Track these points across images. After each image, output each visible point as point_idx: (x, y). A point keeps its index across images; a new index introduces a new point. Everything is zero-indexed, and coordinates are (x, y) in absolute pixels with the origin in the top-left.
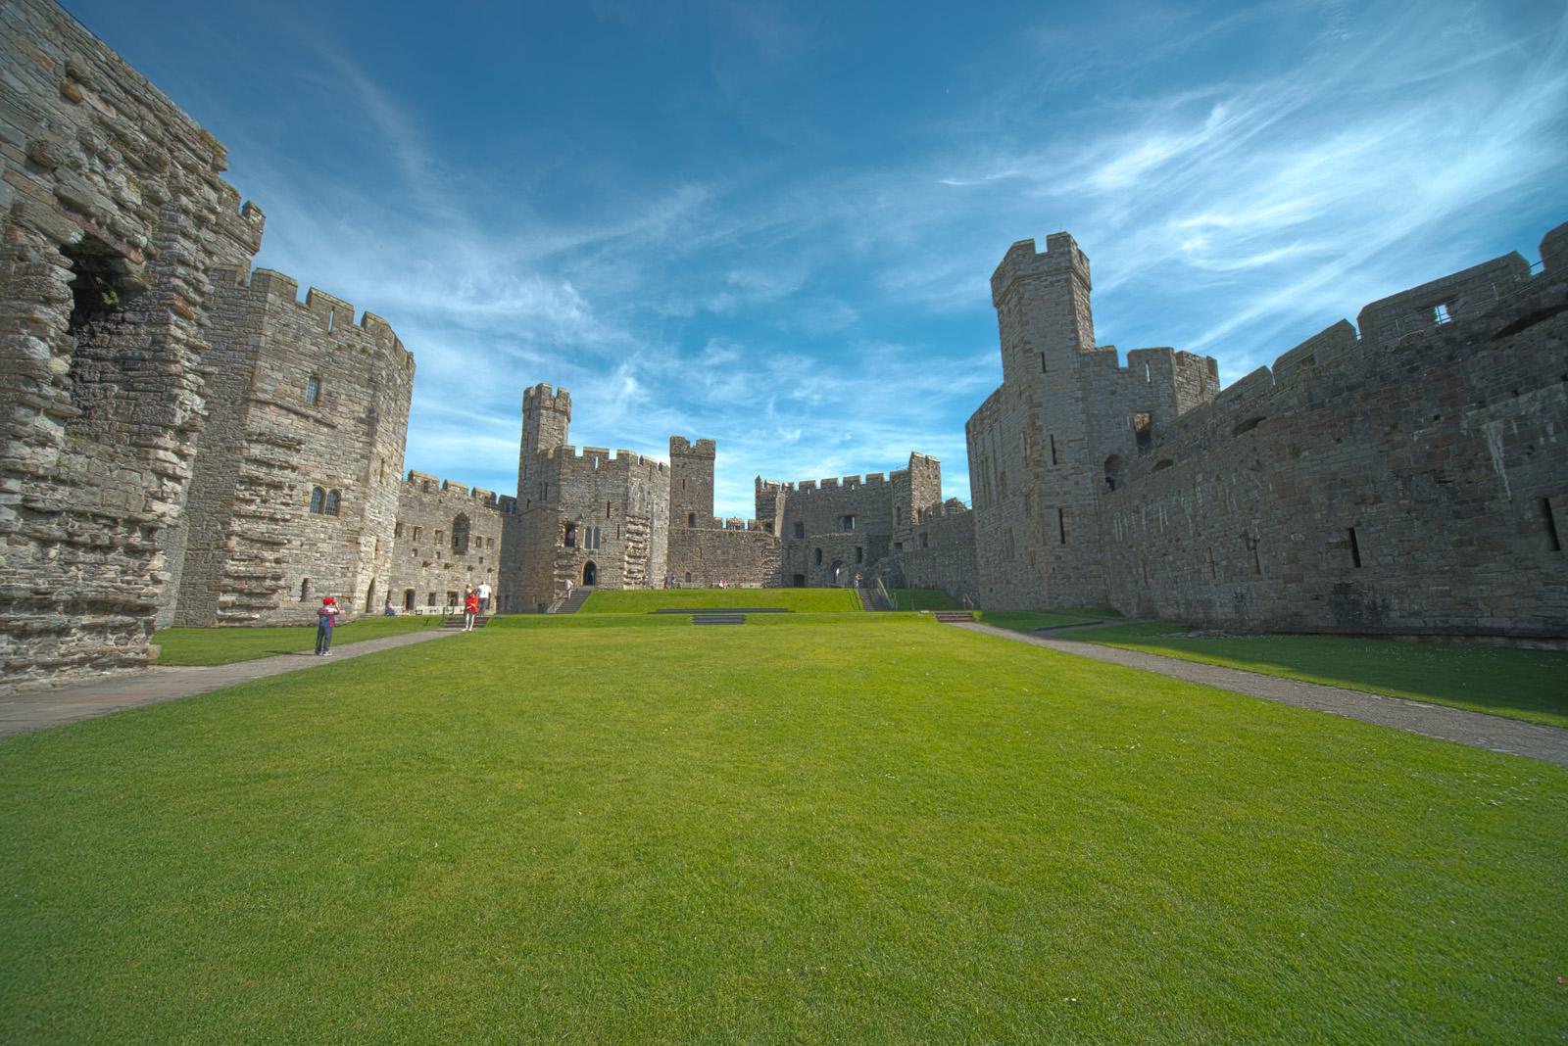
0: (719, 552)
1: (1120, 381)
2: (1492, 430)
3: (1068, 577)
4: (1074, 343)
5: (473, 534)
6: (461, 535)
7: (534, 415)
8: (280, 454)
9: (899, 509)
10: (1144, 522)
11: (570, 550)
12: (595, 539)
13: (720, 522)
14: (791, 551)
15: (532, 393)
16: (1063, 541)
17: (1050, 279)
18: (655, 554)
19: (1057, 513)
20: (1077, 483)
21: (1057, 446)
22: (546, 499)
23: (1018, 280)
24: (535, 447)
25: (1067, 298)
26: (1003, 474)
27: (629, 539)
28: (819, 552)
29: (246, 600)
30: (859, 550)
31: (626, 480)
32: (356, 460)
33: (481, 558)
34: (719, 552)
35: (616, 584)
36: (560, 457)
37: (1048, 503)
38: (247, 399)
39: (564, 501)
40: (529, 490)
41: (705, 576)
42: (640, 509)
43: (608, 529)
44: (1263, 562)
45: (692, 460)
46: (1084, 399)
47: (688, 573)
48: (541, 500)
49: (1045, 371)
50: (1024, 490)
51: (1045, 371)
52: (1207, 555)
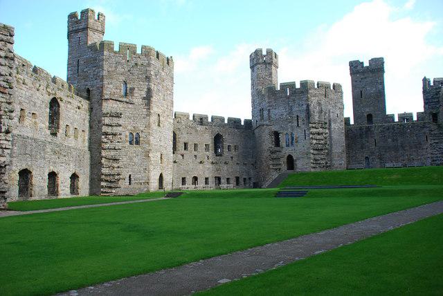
0: (390, 140)
5: (226, 144)
8: (115, 121)
11: (277, 149)
12: (292, 141)
13: (392, 117)
18: (334, 147)
27: (312, 139)
29: (109, 185)
31: (307, 100)
32: (144, 118)
33: (232, 157)
34: (390, 140)
35: (306, 168)
38: (101, 99)
41: (381, 159)
43: (298, 133)
47: (366, 158)
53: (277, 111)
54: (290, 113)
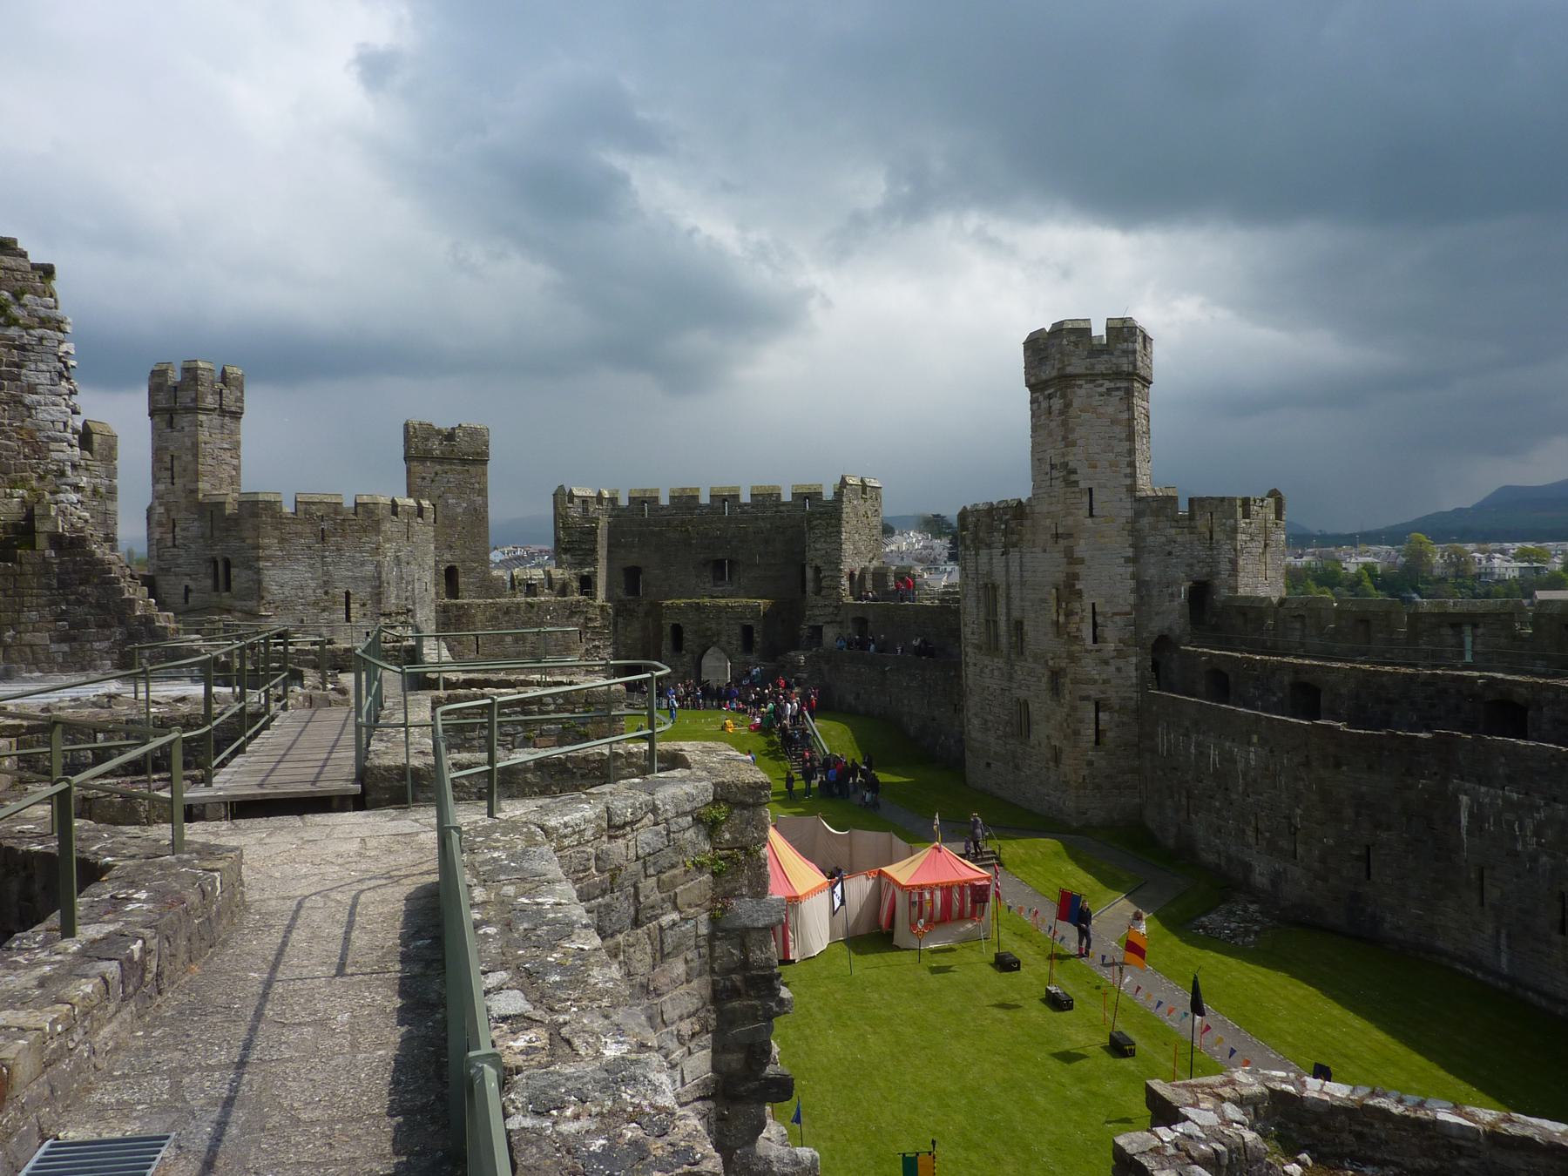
1: (1179, 539)
2: (1464, 799)
3: (1098, 787)
4: (1128, 482)
6: (350, 803)
7: (183, 421)
9: (818, 570)
10: (1193, 750)
14: (620, 620)
15: (175, 376)
16: (1097, 742)
17: (1108, 384)
19: (1092, 707)
20: (1119, 670)
21: (1099, 620)
22: (228, 588)
23: (1065, 381)
24: (191, 486)
25: (1125, 416)
26: (1019, 625)
28: (677, 631)
30: (747, 631)
36: (256, 515)
37: (1084, 694)
39: (269, 598)
40: (186, 569)
42: (398, 597)
44: (1300, 850)
45: (447, 467)
46: (1134, 560)
48: (216, 588)
49: (1091, 515)
50: (1051, 663)
51: (1091, 515)
52: (1252, 819)
53: (287, 575)
54: (326, 585)
